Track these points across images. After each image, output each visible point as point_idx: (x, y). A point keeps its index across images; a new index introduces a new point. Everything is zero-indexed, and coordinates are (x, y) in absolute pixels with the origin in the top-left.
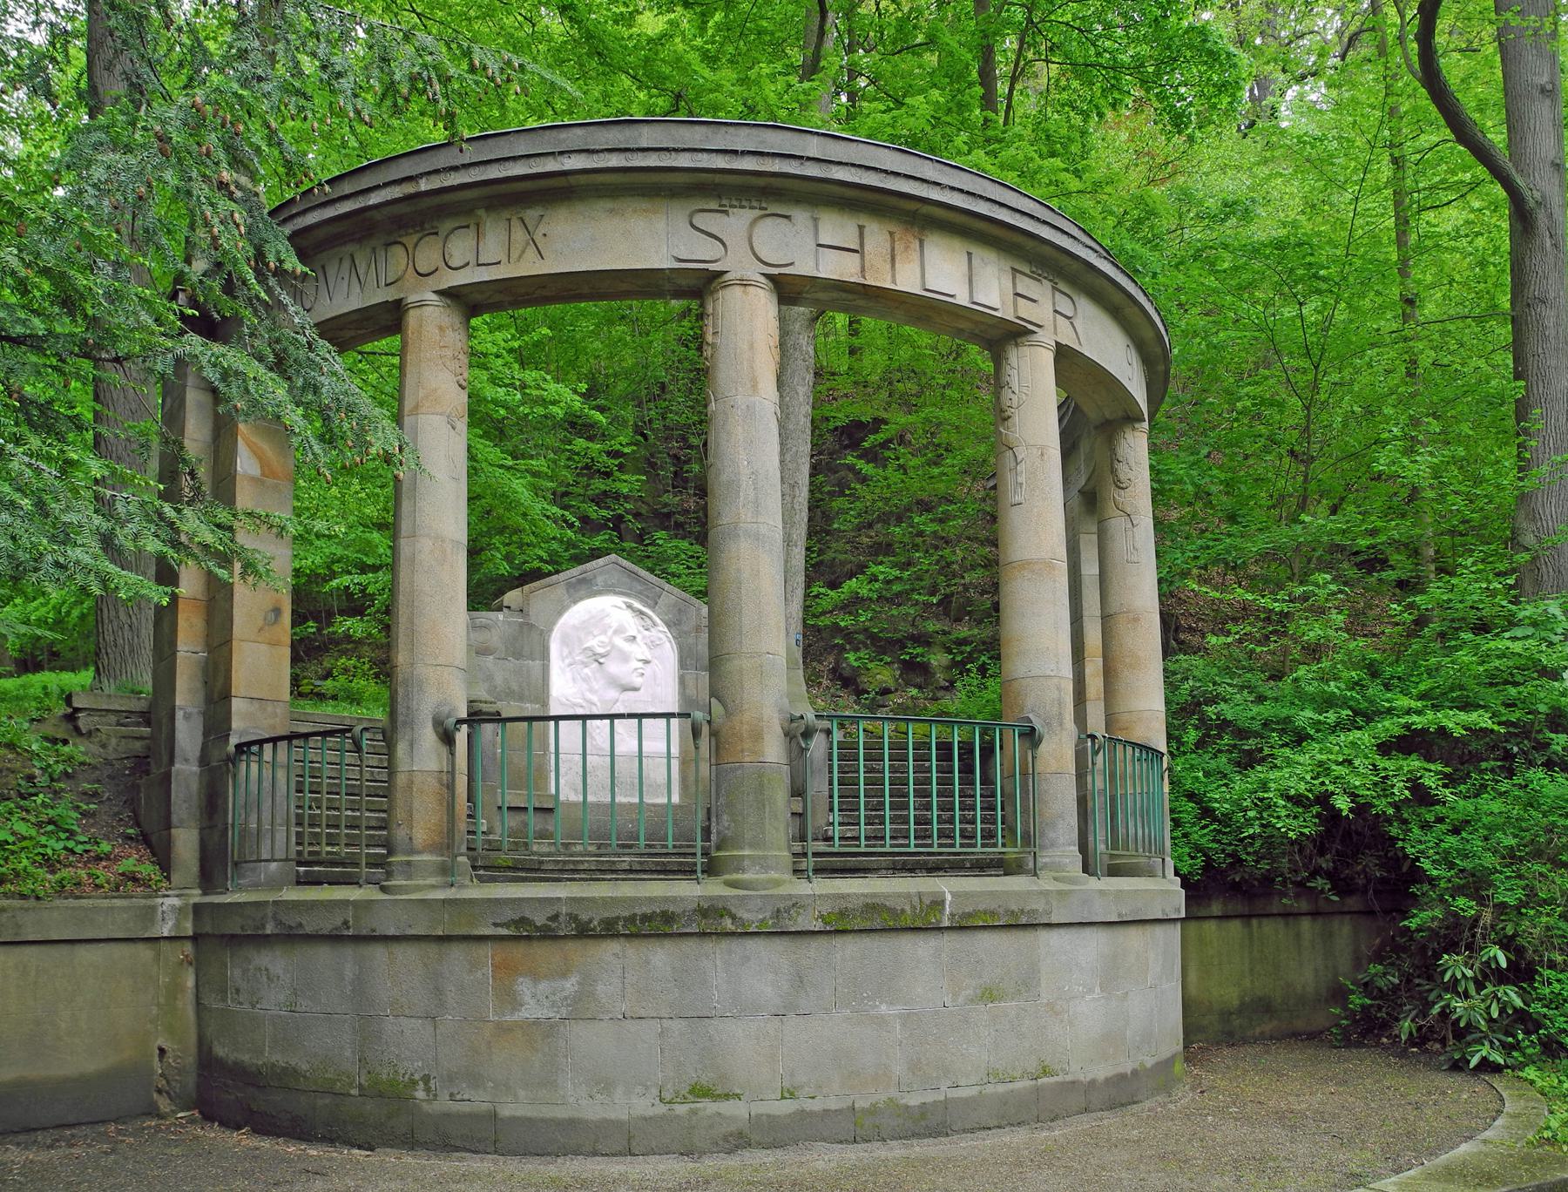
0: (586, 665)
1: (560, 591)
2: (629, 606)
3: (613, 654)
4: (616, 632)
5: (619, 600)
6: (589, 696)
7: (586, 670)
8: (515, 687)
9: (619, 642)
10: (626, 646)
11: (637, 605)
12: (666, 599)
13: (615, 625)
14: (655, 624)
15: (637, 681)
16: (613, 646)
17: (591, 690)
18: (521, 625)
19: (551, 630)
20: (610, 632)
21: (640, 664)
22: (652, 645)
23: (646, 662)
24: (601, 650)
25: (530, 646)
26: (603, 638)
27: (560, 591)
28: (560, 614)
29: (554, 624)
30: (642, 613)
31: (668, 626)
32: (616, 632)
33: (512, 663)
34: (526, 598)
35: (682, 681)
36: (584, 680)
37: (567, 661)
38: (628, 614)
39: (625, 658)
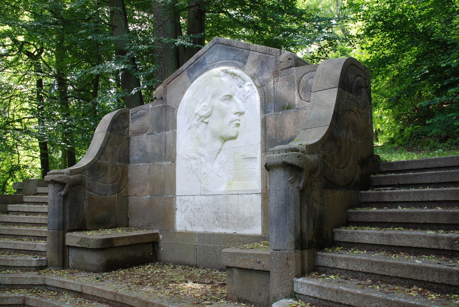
0: (197, 126)
2: (226, 72)
3: (215, 113)
4: (214, 96)
6: (201, 150)
7: (198, 130)
8: (157, 150)
9: (217, 102)
11: (232, 69)
12: (253, 56)
16: (213, 108)
17: (202, 145)
19: (178, 107)
20: (209, 98)
21: (236, 117)
23: (241, 114)
24: (204, 113)
27: (185, 77)
29: (179, 102)
31: (253, 77)
32: (214, 96)
33: (157, 135)
34: (165, 91)
37: (188, 126)
38: (226, 79)
39: (223, 114)
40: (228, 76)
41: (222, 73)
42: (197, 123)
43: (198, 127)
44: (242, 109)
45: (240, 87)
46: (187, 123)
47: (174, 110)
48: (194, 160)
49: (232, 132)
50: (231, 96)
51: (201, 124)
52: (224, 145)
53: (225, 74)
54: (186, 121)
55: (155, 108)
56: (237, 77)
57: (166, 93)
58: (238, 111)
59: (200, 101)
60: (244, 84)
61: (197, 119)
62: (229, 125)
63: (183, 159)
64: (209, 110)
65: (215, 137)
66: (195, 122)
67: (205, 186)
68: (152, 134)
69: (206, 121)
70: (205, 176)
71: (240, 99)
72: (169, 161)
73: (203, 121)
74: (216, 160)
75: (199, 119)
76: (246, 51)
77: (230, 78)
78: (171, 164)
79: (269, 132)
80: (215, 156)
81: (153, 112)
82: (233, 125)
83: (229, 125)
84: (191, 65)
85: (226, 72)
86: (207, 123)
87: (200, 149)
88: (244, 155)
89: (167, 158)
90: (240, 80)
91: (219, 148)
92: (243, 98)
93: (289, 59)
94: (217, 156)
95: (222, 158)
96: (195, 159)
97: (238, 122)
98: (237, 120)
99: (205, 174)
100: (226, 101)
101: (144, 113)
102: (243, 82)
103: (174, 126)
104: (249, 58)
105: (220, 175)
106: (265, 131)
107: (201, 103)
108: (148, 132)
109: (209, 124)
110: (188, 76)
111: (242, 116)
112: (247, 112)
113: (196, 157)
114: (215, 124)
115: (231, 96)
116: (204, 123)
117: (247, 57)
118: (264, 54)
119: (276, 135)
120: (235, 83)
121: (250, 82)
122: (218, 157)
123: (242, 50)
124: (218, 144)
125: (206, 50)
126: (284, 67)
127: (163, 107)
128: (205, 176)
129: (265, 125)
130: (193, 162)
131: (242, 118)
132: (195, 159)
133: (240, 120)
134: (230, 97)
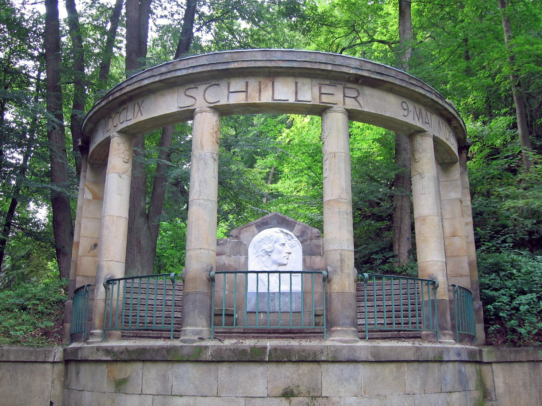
1: (254, 228)
2: (282, 232)
3: (275, 251)
5: (277, 229)
7: (263, 258)
9: (277, 246)
10: (281, 248)
11: (285, 231)
13: (275, 240)
14: (292, 238)
15: (285, 262)
18: (237, 242)
21: (287, 255)
22: (292, 246)
23: (290, 253)
24: (269, 250)
25: (241, 249)
26: (270, 245)
28: (253, 237)
30: (287, 234)
31: (298, 237)
32: (275, 242)
36: (262, 262)
37: (256, 255)
38: (281, 235)
39: (280, 252)
41: (280, 232)
44: (290, 251)
50: (284, 244)
55: (232, 242)
66: (262, 253)
69: (270, 254)
82: (285, 258)
85: (282, 232)
86: (270, 255)
90: (290, 237)
103: (246, 254)
114: (274, 256)
115: (284, 244)
116: (267, 256)
121: (296, 239)
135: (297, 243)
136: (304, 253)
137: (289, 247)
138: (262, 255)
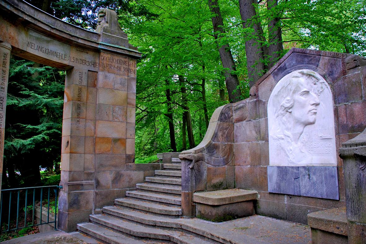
1: (271, 78)
2: (303, 74)
3: (296, 105)
5: (296, 73)
7: (284, 118)
10: (303, 98)
13: (293, 88)
14: (318, 80)
16: (294, 101)
17: (288, 129)
21: (313, 107)
22: (319, 93)
23: (317, 105)
24: (288, 105)
27: (271, 78)
30: (310, 75)
31: (324, 77)
32: (294, 92)
34: (257, 90)
35: (336, 112)
37: (276, 115)
38: (303, 80)
39: (303, 106)
40: (305, 76)
41: (300, 75)
42: (283, 112)
43: (284, 116)
44: (318, 101)
45: (315, 84)
46: (275, 112)
47: (265, 104)
48: (282, 140)
49: (311, 118)
51: (286, 113)
52: (305, 129)
53: (302, 75)
54: (275, 111)
56: (312, 77)
57: (258, 90)
58: (314, 102)
59: (284, 96)
60: (318, 82)
61: (283, 109)
62: (308, 113)
63: (274, 139)
64: (292, 103)
65: (297, 122)
67: (292, 160)
68: (249, 121)
69: (290, 111)
70: (291, 152)
71: (315, 93)
72: (263, 141)
73: (287, 111)
74: (299, 140)
75: (284, 110)
76: (317, 57)
77: (306, 78)
78: (265, 143)
79: (340, 119)
80: (298, 137)
81: (250, 105)
82: (310, 114)
83: (308, 113)
84: (275, 70)
85: (303, 74)
86: (290, 112)
87: (287, 132)
88: (321, 137)
89: (262, 138)
91: (301, 131)
92: (318, 93)
93: (355, 60)
94: (299, 137)
95: (303, 138)
96: (282, 139)
97: (314, 111)
98: (314, 109)
99: (291, 150)
100: (304, 96)
101: (243, 106)
102: (317, 81)
103: (266, 115)
104: (320, 62)
105: (303, 151)
106: (338, 118)
107: (285, 98)
108: (246, 120)
109: (292, 113)
110: (274, 77)
111: (318, 106)
112: (321, 103)
113: (284, 138)
114: (297, 113)
116: (288, 113)
117: (319, 61)
118: (332, 58)
119: (347, 121)
120: (311, 81)
122: (300, 138)
123: (314, 56)
124: (299, 128)
125: (286, 58)
126: (350, 67)
127: (256, 101)
128: (291, 152)
129: (338, 113)
130: (282, 141)
131: (319, 108)
132: (282, 139)
133: (316, 110)
134: (307, 92)
135: (324, 86)
136: (336, 98)
137: (315, 95)
138: (282, 114)
